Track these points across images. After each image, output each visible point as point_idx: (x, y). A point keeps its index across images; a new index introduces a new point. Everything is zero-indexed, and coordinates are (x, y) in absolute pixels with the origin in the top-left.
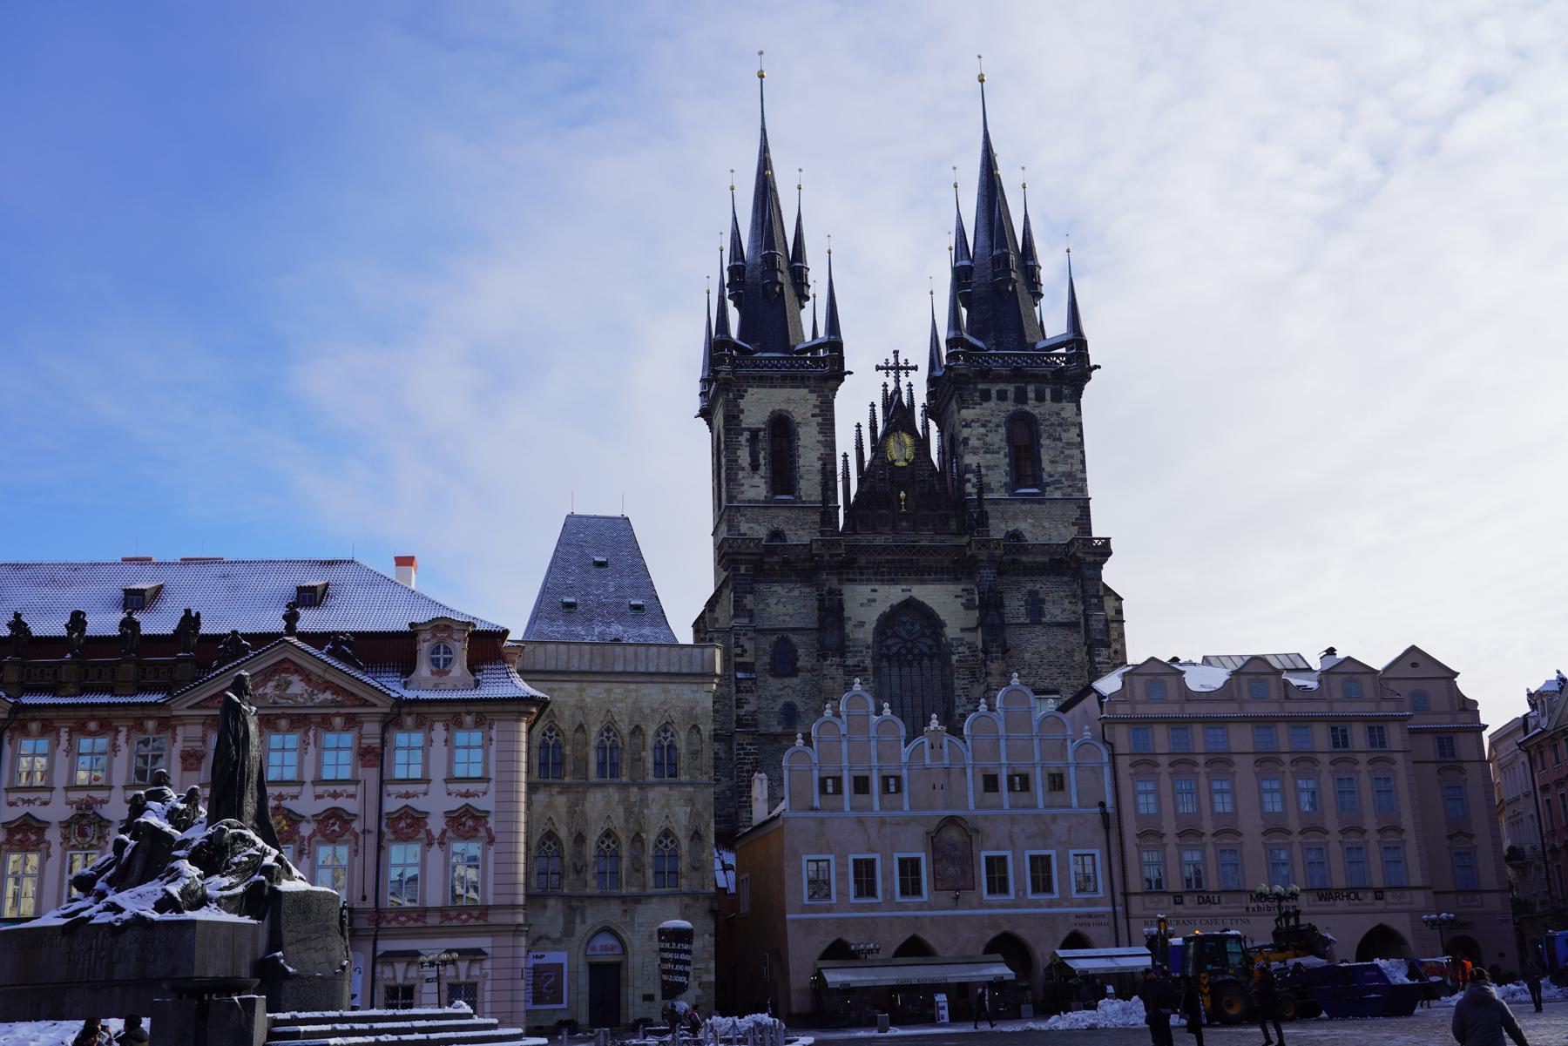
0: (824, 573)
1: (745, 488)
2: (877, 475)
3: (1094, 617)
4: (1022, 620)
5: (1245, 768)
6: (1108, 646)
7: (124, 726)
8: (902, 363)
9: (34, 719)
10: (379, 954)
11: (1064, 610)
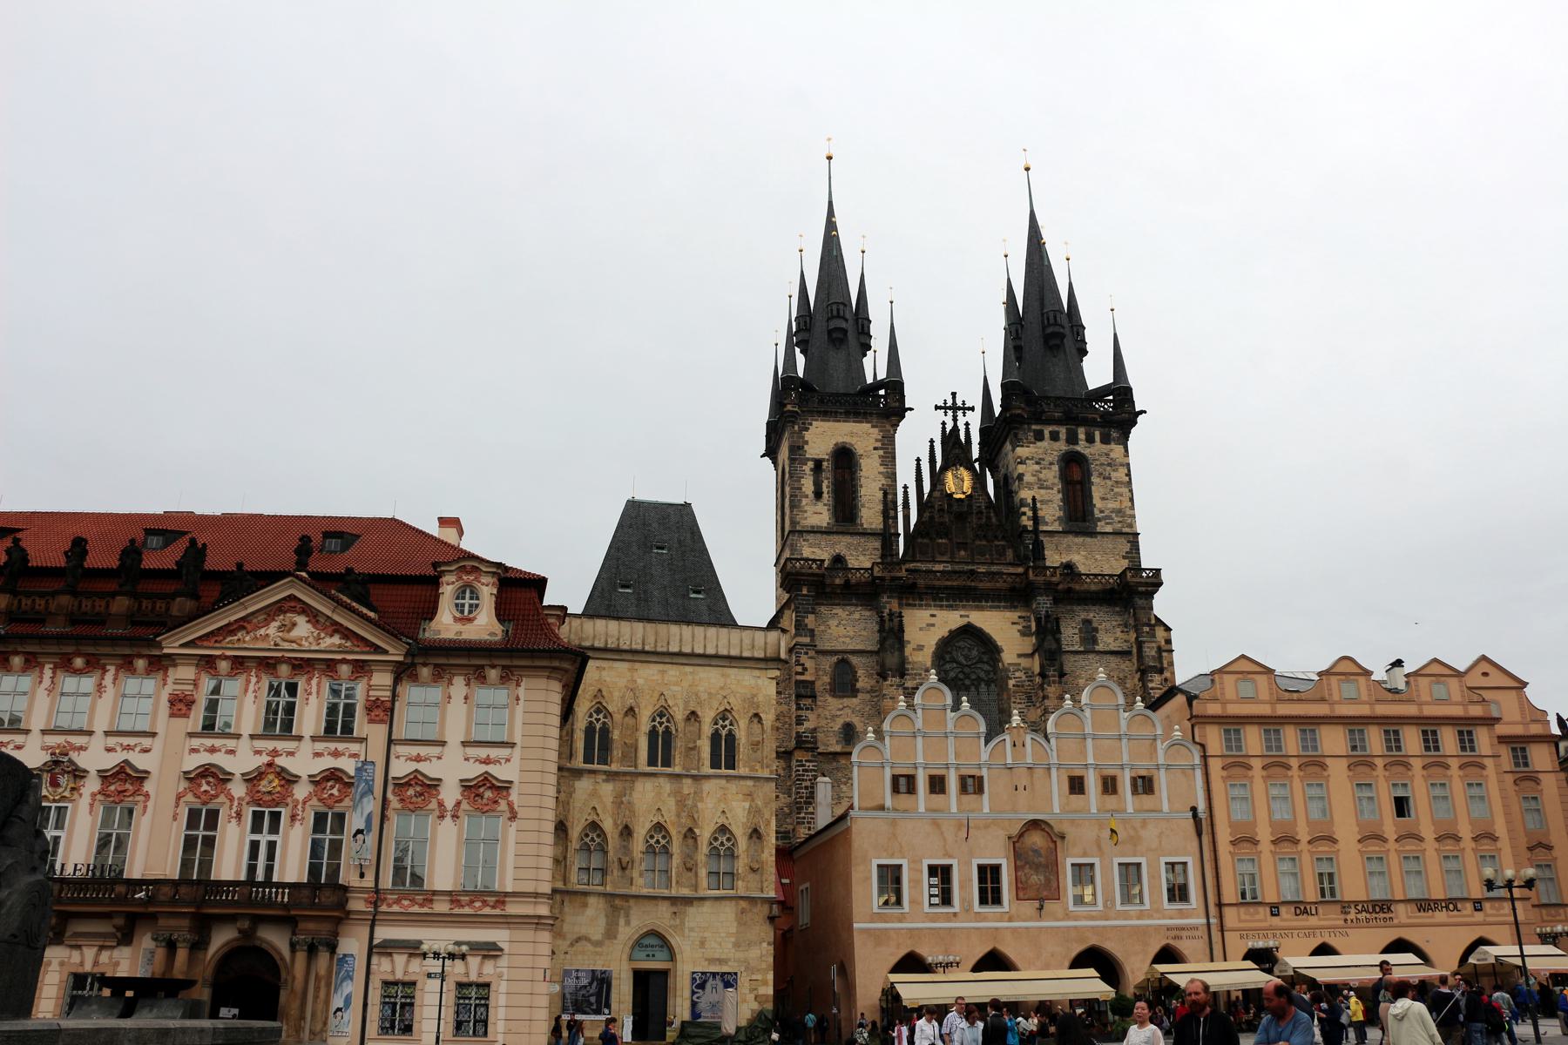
0: (885, 597)
2: (936, 505)
3: (1146, 645)
4: (1076, 648)
5: (1338, 771)
6: (1161, 671)
7: (111, 664)
8: (959, 403)
9: (17, 653)
10: (376, 942)
11: (1116, 639)
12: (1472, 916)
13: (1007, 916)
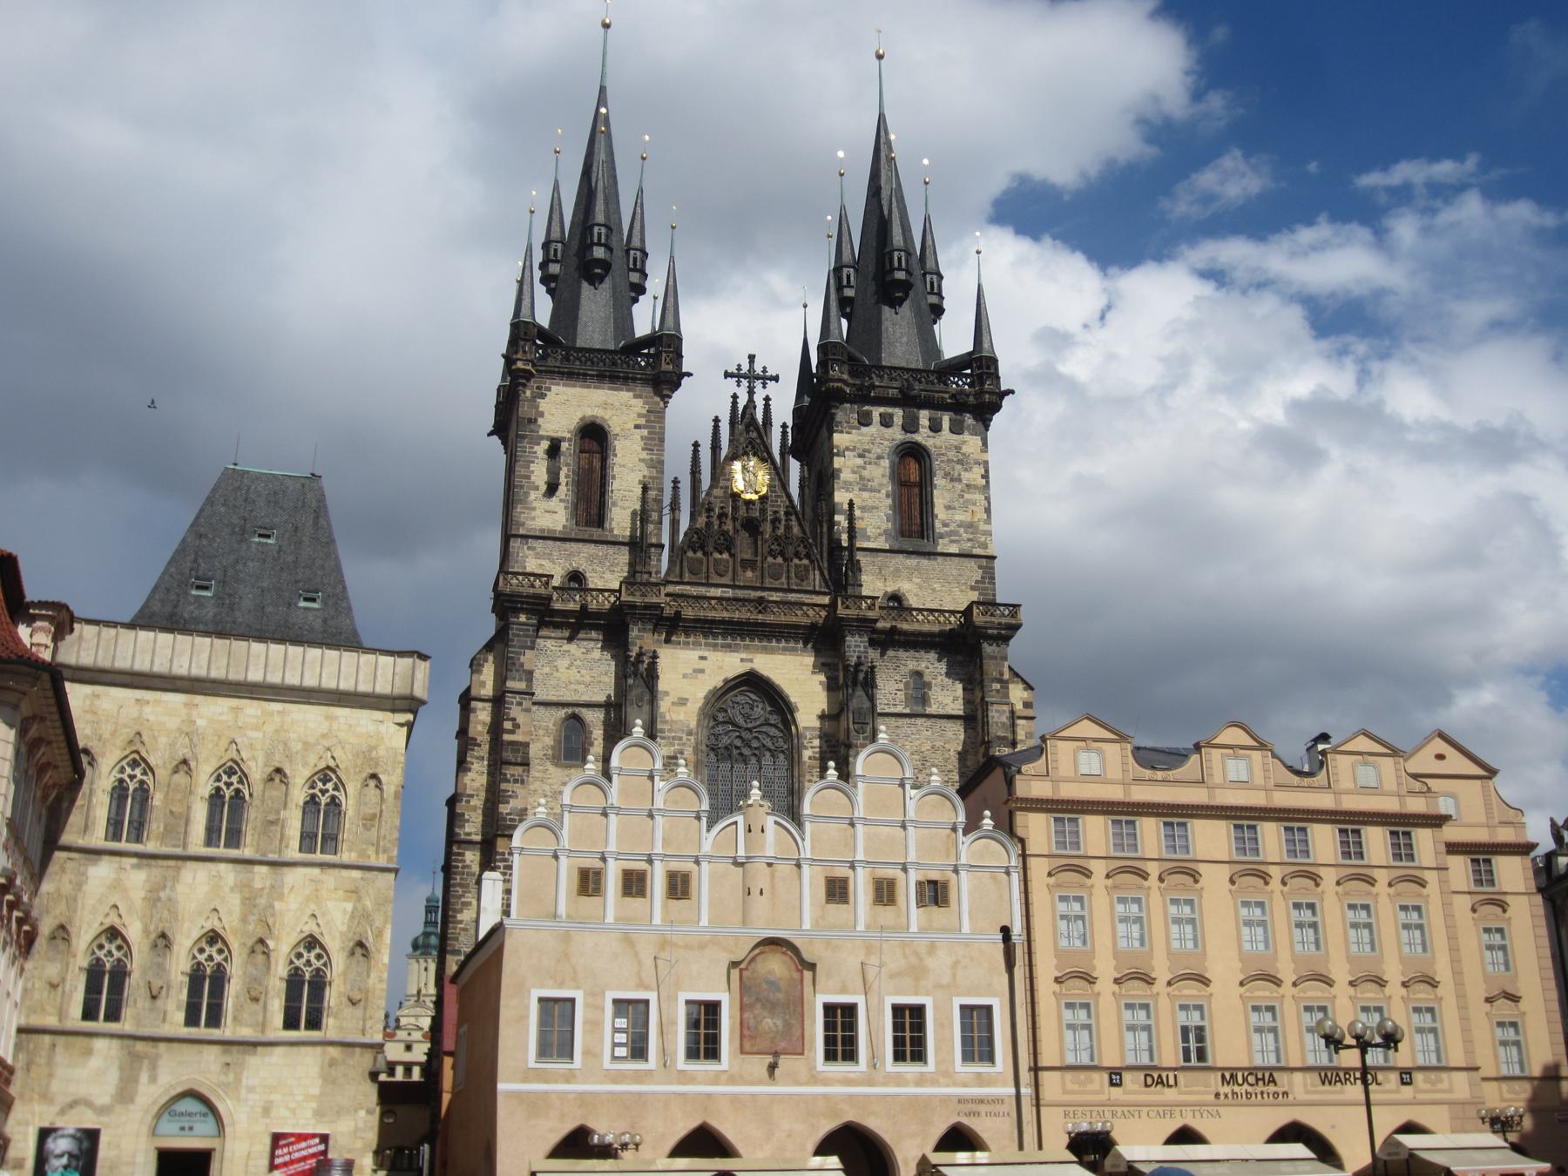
1: (537, 512)
3: (995, 707)
4: (900, 709)
5: (1215, 879)
8: (758, 369)
12: (1398, 1092)
13: (724, 1077)
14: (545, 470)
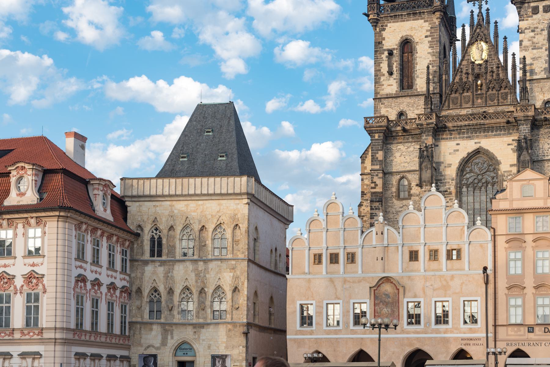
14: (387, 66)
